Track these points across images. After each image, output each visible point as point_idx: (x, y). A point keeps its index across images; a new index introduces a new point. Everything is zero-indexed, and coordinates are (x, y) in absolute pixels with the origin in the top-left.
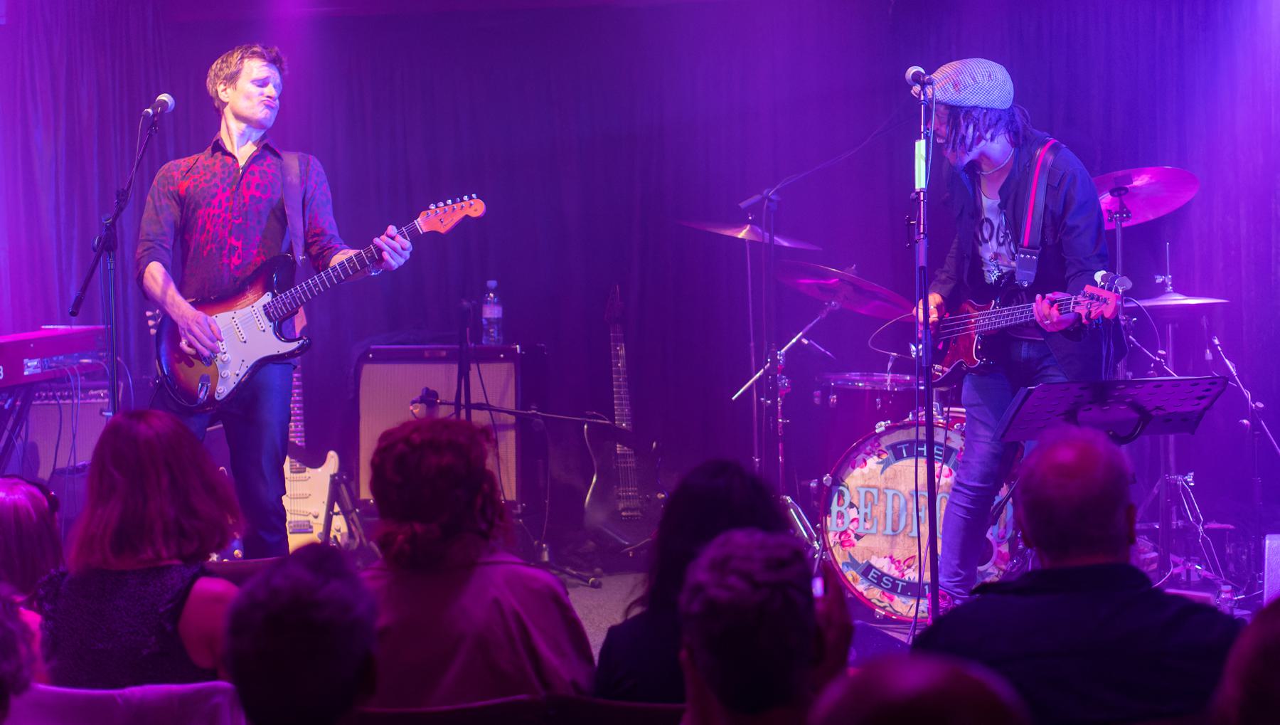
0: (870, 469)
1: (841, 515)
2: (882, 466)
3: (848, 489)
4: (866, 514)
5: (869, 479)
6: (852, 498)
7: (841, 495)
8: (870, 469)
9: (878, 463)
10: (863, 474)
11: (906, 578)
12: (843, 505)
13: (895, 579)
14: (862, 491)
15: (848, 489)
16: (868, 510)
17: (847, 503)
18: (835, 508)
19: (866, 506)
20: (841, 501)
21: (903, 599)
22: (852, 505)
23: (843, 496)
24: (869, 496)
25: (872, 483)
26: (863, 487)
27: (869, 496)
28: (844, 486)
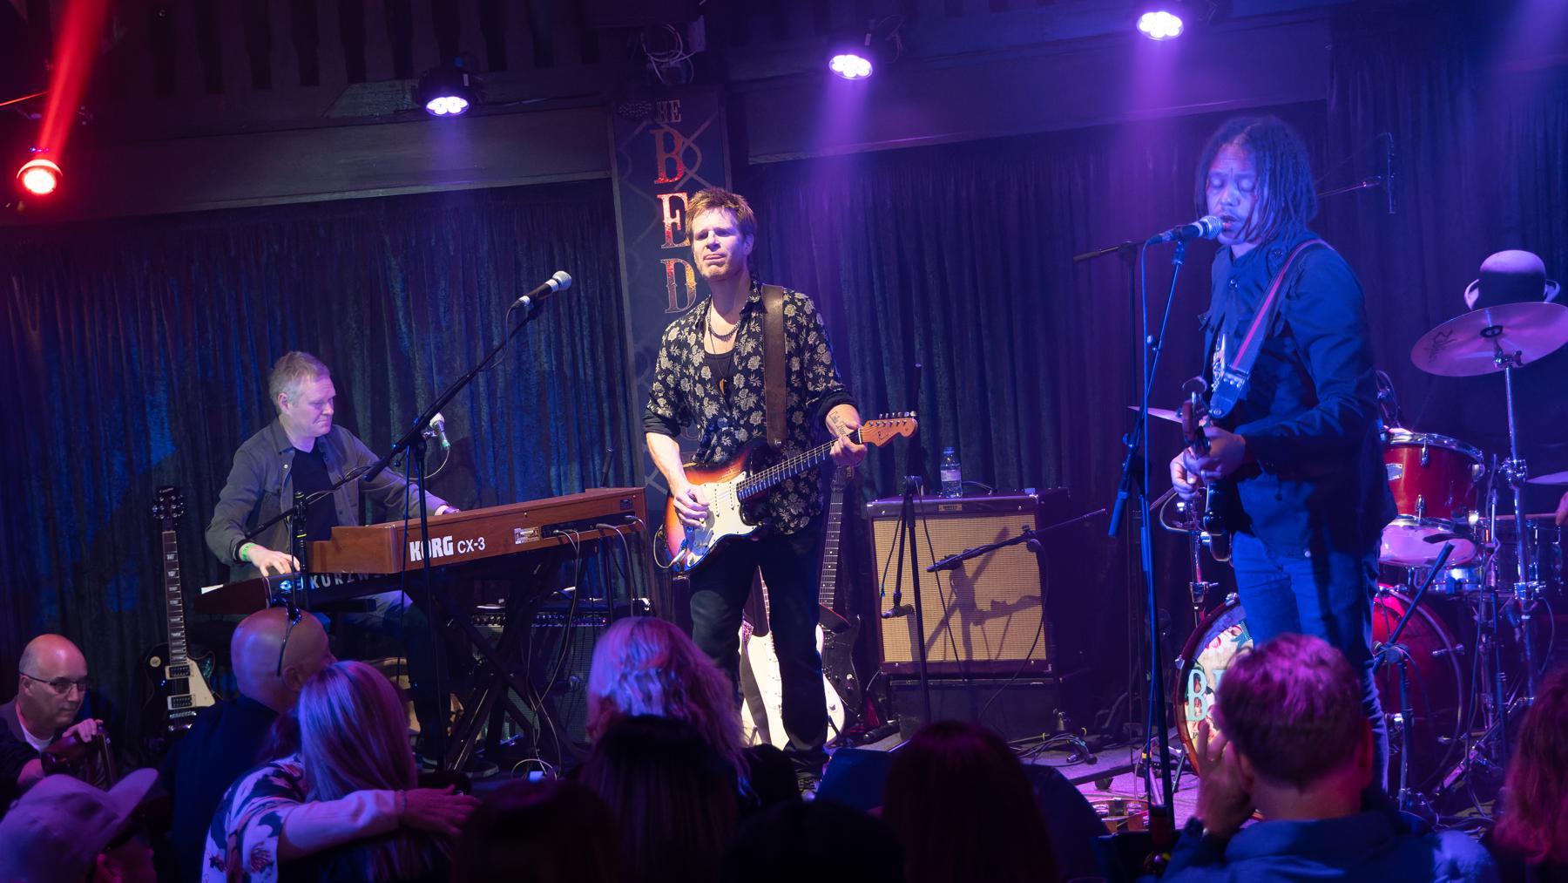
0: (1225, 649)
1: (1198, 702)
2: (1236, 644)
3: (1203, 672)
6: (1208, 682)
7: (1197, 677)
8: (1225, 649)
9: (1233, 641)
10: (1218, 655)
12: (1199, 691)
15: (1203, 672)
17: (1204, 689)
18: (1191, 694)
20: (1198, 686)
22: (1209, 691)
23: (1200, 680)
28: (1198, 668)
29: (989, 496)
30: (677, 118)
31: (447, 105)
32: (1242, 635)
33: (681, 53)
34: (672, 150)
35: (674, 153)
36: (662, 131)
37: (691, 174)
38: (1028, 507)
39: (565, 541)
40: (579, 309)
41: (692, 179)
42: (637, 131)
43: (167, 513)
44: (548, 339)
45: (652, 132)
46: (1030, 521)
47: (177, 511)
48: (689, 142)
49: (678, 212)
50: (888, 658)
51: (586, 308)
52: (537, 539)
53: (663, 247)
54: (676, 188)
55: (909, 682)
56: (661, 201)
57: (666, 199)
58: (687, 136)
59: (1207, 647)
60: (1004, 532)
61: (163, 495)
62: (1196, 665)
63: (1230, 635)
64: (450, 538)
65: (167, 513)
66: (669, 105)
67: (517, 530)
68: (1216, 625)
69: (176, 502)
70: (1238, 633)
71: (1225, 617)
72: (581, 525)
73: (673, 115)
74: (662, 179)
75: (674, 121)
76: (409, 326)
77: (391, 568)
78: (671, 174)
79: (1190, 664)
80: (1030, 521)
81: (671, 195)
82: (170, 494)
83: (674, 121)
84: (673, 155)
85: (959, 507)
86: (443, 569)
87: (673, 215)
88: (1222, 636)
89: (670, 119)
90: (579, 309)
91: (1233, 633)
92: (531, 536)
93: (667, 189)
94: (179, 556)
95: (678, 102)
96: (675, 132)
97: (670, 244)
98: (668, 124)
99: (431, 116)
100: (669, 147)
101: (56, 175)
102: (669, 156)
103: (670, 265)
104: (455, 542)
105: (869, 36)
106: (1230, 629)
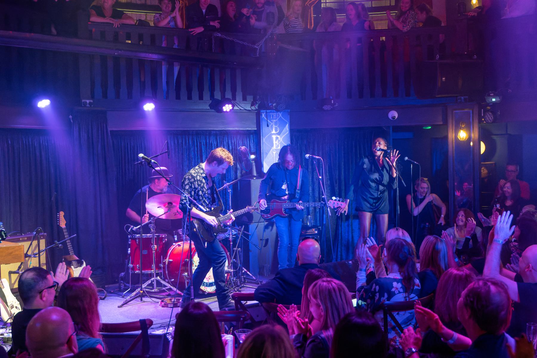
11: (209, 282)
13: (207, 283)
17: (195, 266)
18: (193, 268)
21: (209, 288)
59: (194, 256)
85: (26, 239)
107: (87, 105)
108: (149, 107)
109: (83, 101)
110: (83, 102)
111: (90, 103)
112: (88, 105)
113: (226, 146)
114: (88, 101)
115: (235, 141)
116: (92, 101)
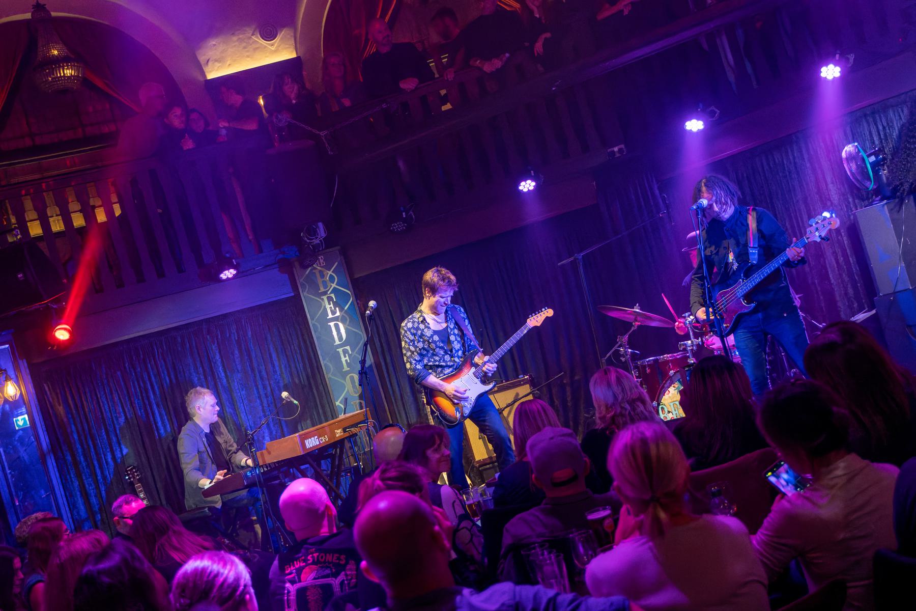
4: (676, 414)
5: (673, 398)
6: (668, 408)
7: (662, 408)
10: (670, 397)
14: (672, 404)
16: (677, 412)
17: (667, 412)
19: (675, 411)
20: (664, 412)
22: (669, 412)
24: (675, 406)
25: (675, 400)
26: (671, 402)
27: (675, 406)
29: (502, 382)
30: (323, 264)
31: (229, 274)
32: (678, 387)
33: (319, 237)
34: (323, 278)
35: (325, 278)
36: (316, 270)
37: (334, 285)
38: (525, 382)
39: (354, 433)
40: (296, 352)
41: (334, 287)
42: (307, 273)
43: (134, 478)
44: (285, 367)
45: (314, 271)
46: (528, 386)
47: (138, 475)
48: (330, 273)
49: (331, 302)
50: (477, 459)
51: (298, 352)
52: (342, 434)
53: (328, 318)
54: (329, 293)
55: (488, 466)
56: (323, 299)
57: (325, 298)
58: (329, 271)
59: (664, 395)
60: (517, 394)
61: (130, 470)
62: (661, 404)
63: (674, 388)
64: (316, 437)
65: (134, 478)
66: (319, 260)
67: (336, 431)
68: (666, 386)
69: (136, 472)
70: (676, 386)
71: (669, 381)
72: (355, 425)
73: (322, 264)
74: (322, 290)
75: (322, 265)
76: (225, 372)
77: (299, 452)
78: (325, 287)
79: (659, 405)
80: (528, 386)
81: (327, 296)
82: (132, 469)
83: (322, 265)
84: (324, 279)
86: (316, 451)
87: (330, 304)
88: (669, 389)
89: (320, 264)
90: (296, 352)
91: (674, 387)
92: (341, 433)
93: (325, 293)
94: (146, 493)
95: (322, 257)
96: (323, 269)
97: (330, 316)
98: (320, 267)
99: (221, 280)
100: (323, 276)
101: (65, 329)
102: (323, 280)
103: (332, 324)
104: (318, 438)
105: (404, 214)
106: (673, 385)
107: (615, 155)
108: (694, 125)
109: (609, 150)
110: (610, 152)
111: (620, 150)
112: (618, 155)
113: (868, 140)
114: (616, 149)
115: (885, 124)
116: (622, 146)
